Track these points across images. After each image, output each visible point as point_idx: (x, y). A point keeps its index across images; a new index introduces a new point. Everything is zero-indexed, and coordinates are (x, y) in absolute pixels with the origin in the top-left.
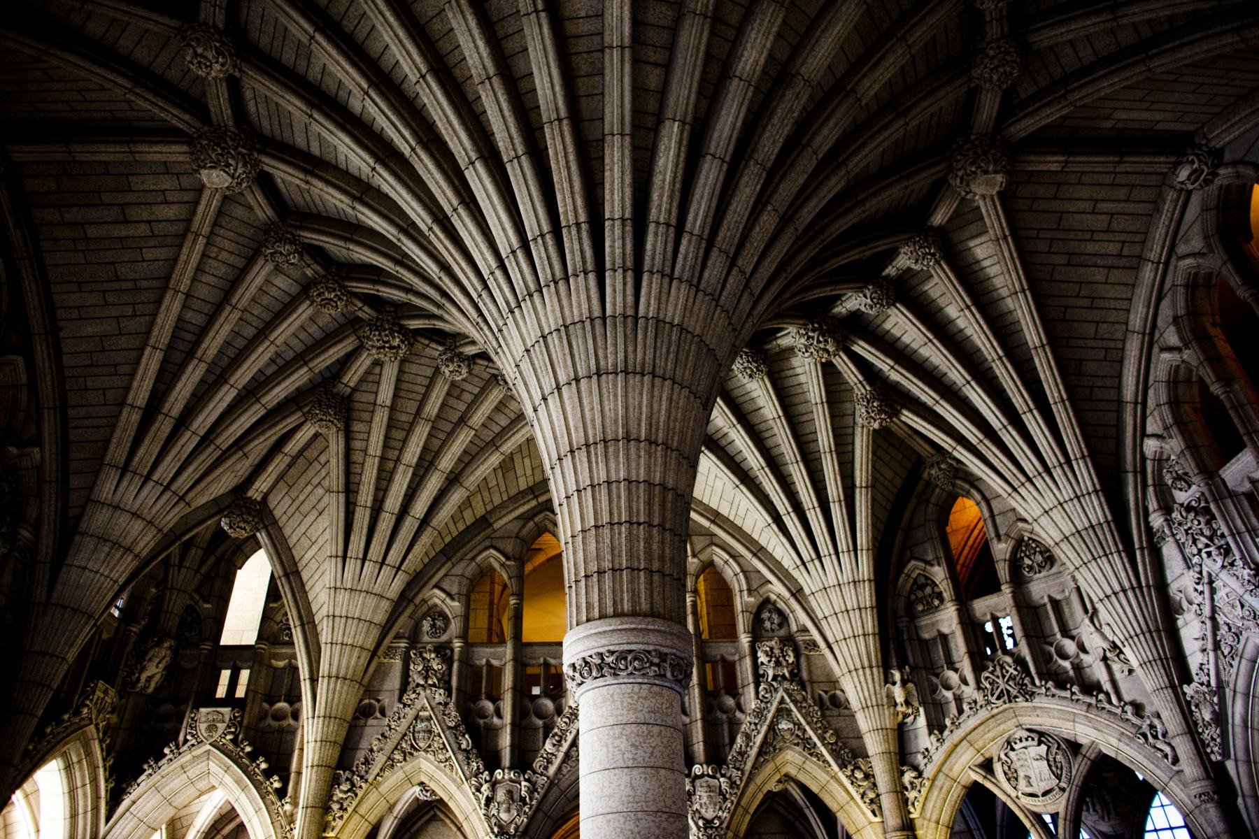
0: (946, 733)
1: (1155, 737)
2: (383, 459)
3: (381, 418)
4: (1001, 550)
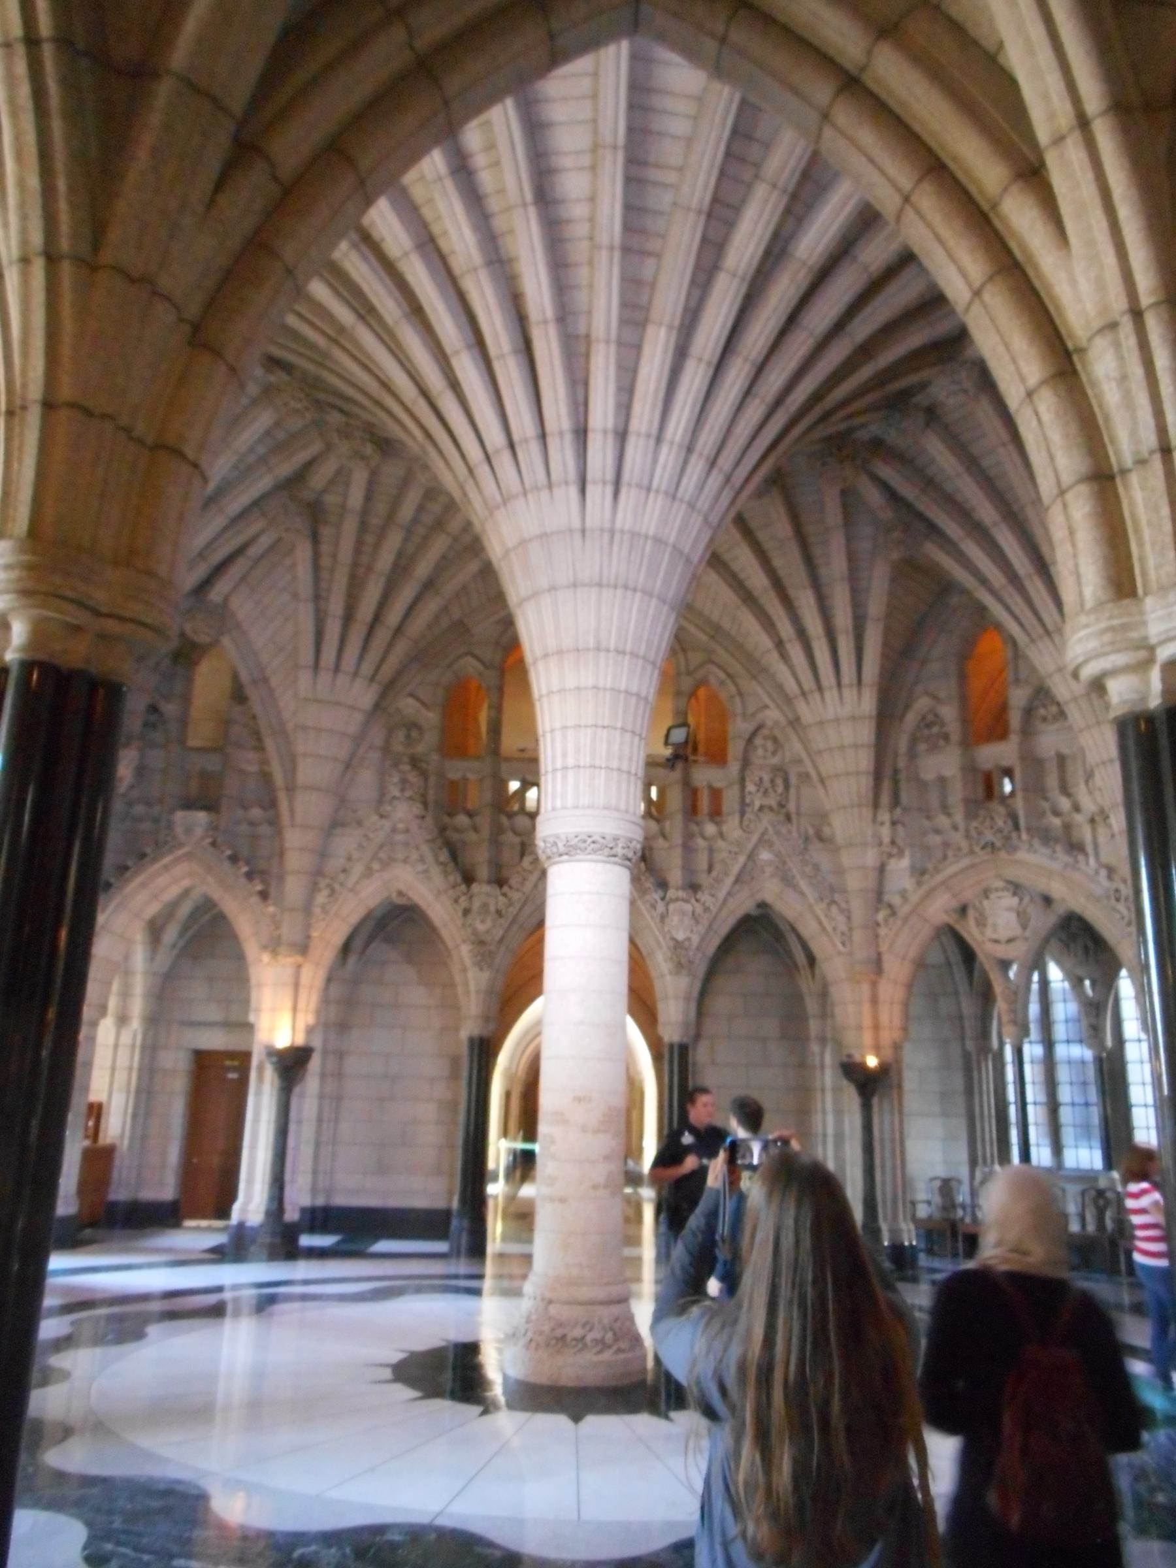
2: (355, 565)
3: (350, 526)
4: (1018, 697)
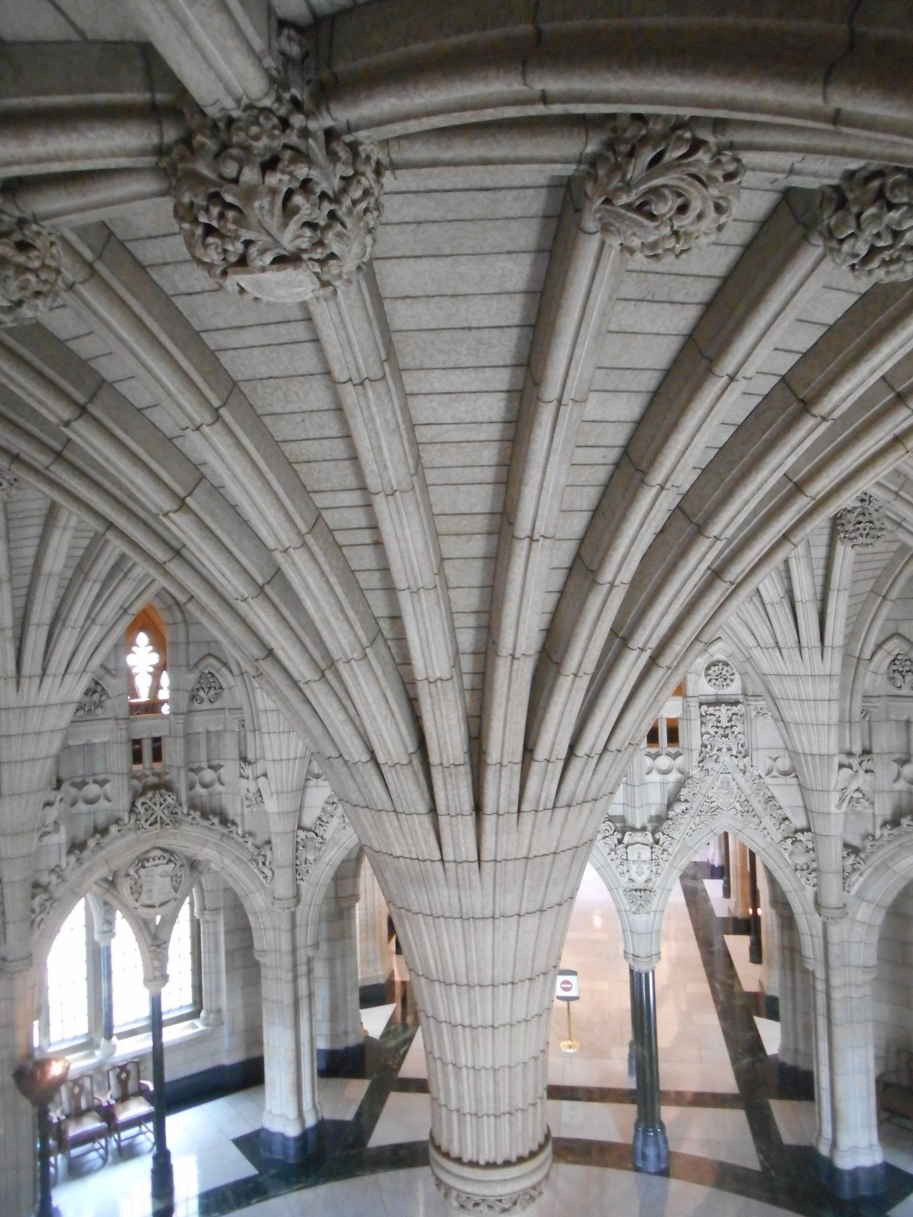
0: (86, 853)
1: (264, 863)
